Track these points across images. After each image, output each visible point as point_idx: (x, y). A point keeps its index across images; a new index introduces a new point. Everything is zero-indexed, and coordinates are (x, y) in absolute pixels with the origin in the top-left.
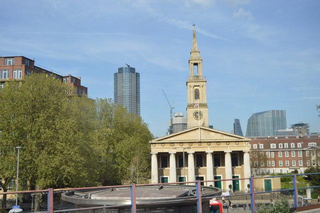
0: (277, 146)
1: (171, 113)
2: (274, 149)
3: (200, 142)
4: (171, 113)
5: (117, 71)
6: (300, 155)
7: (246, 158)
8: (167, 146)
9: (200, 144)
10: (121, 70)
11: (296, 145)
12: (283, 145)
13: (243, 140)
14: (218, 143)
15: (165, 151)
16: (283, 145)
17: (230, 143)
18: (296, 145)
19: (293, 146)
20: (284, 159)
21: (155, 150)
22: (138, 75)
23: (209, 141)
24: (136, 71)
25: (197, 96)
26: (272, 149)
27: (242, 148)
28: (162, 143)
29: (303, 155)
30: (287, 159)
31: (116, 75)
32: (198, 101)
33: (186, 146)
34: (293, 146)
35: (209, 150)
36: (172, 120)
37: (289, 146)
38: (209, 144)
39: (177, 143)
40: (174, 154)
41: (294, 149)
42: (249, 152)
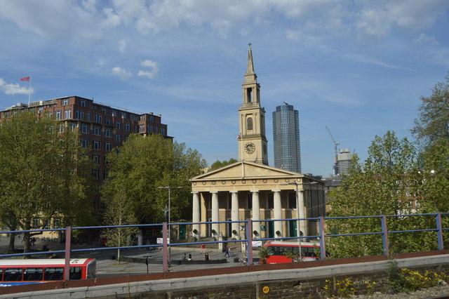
1: (336, 149)
3: (245, 180)
4: (336, 149)
5: (275, 110)
7: (300, 198)
8: (208, 184)
10: (279, 108)
14: (265, 181)
15: (207, 190)
17: (279, 180)
21: (196, 189)
22: (296, 112)
24: (294, 109)
25: (250, 126)
31: (274, 113)
32: (250, 132)
33: (229, 184)
35: (254, 189)
36: (337, 156)
38: (254, 181)
39: (218, 181)
42: (302, 192)
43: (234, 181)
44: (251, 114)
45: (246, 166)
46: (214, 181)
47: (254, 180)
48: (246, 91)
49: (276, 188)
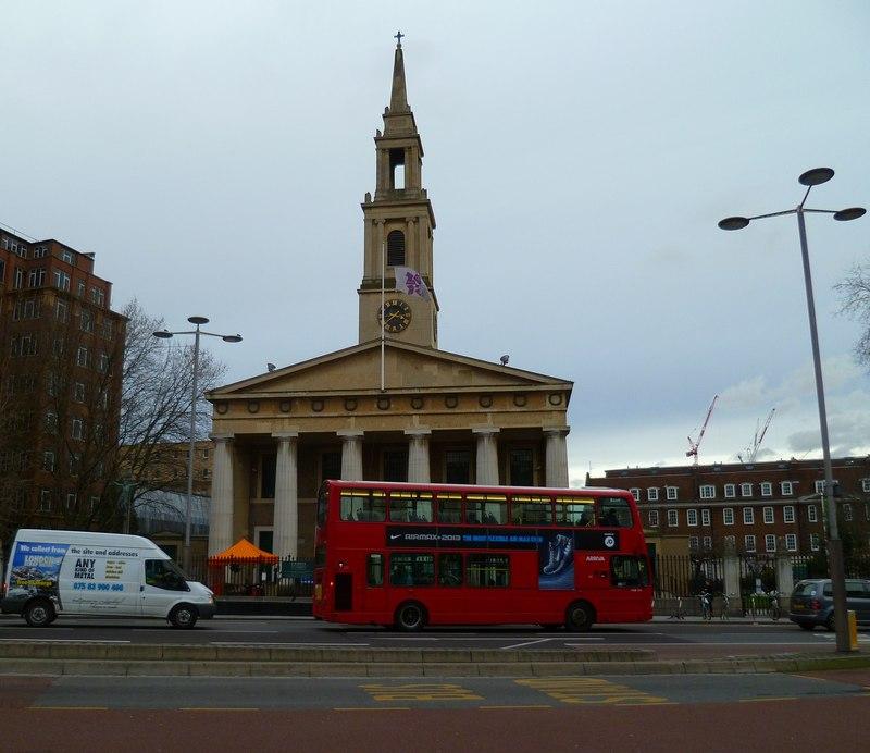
0: (720, 492)
2: (712, 501)
6: (790, 518)
9: (384, 404)
11: (777, 490)
12: (739, 491)
13: (543, 388)
15: (262, 428)
16: (739, 491)
18: (777, 490)
19: (767, 491)
20: (740, 530)
23: (417, 391)
26: (704, 501)
27: (537, 416)
28: (250, 402)
29: (798, 517)
30: (749, 529)
34: (767, 491)
37: (757, 491)
39: (302, 399)
40: (293, 439)
41: (769, 498)
43: (351, 402)
44: (402, 220)
45: (394, 361)
46: (286, 403)
47: (418, 400)
48: (388, 156)
49: (486, 424)
